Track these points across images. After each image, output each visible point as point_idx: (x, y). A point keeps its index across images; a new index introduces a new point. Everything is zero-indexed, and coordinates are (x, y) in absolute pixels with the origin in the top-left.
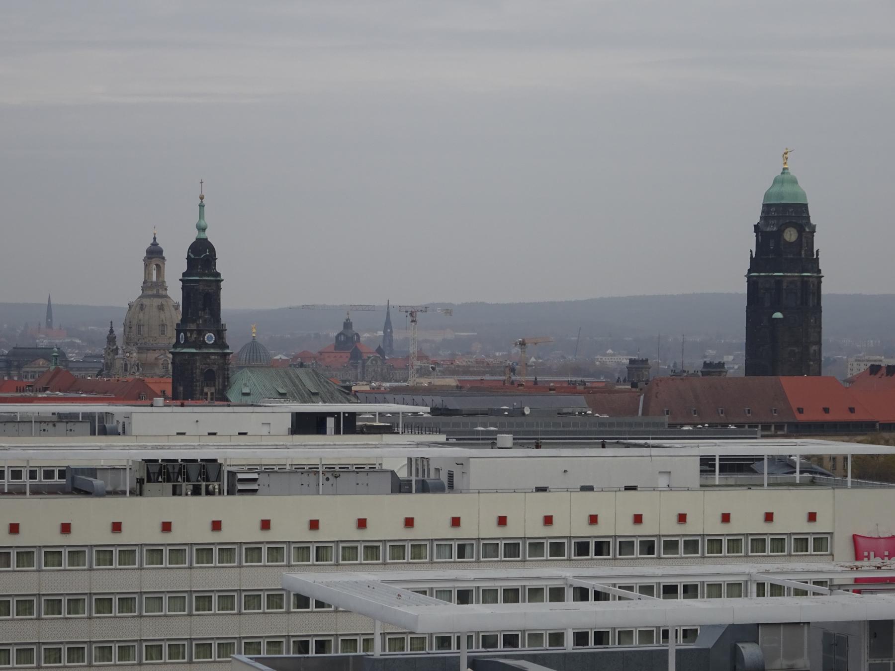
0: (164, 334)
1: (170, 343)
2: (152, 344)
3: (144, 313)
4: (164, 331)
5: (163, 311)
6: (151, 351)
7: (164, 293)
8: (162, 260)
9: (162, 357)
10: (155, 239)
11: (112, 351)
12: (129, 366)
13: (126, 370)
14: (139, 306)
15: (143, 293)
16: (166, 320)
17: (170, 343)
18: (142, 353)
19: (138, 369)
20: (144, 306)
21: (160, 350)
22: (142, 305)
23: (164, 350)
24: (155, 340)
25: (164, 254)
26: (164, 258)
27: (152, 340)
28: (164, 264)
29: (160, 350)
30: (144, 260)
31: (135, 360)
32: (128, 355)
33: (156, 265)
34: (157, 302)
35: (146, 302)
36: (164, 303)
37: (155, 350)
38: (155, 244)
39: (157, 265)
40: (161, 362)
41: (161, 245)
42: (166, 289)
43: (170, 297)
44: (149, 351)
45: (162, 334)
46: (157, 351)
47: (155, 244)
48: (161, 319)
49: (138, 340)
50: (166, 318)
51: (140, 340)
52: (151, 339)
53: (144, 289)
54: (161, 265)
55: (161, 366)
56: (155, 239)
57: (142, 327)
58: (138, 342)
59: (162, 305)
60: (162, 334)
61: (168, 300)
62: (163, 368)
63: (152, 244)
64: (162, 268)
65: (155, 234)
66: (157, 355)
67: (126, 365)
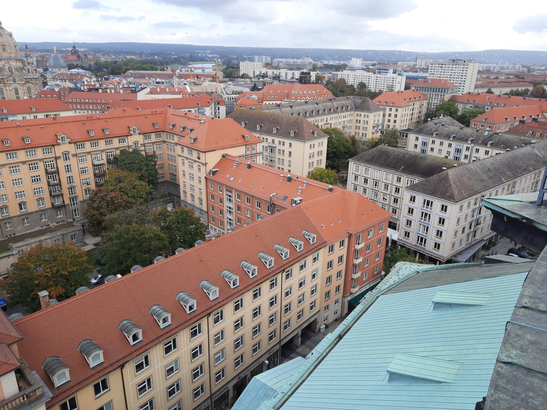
9: (7, 64)
40: (7, 67)
55: (8, 70)
66: (3, 63)
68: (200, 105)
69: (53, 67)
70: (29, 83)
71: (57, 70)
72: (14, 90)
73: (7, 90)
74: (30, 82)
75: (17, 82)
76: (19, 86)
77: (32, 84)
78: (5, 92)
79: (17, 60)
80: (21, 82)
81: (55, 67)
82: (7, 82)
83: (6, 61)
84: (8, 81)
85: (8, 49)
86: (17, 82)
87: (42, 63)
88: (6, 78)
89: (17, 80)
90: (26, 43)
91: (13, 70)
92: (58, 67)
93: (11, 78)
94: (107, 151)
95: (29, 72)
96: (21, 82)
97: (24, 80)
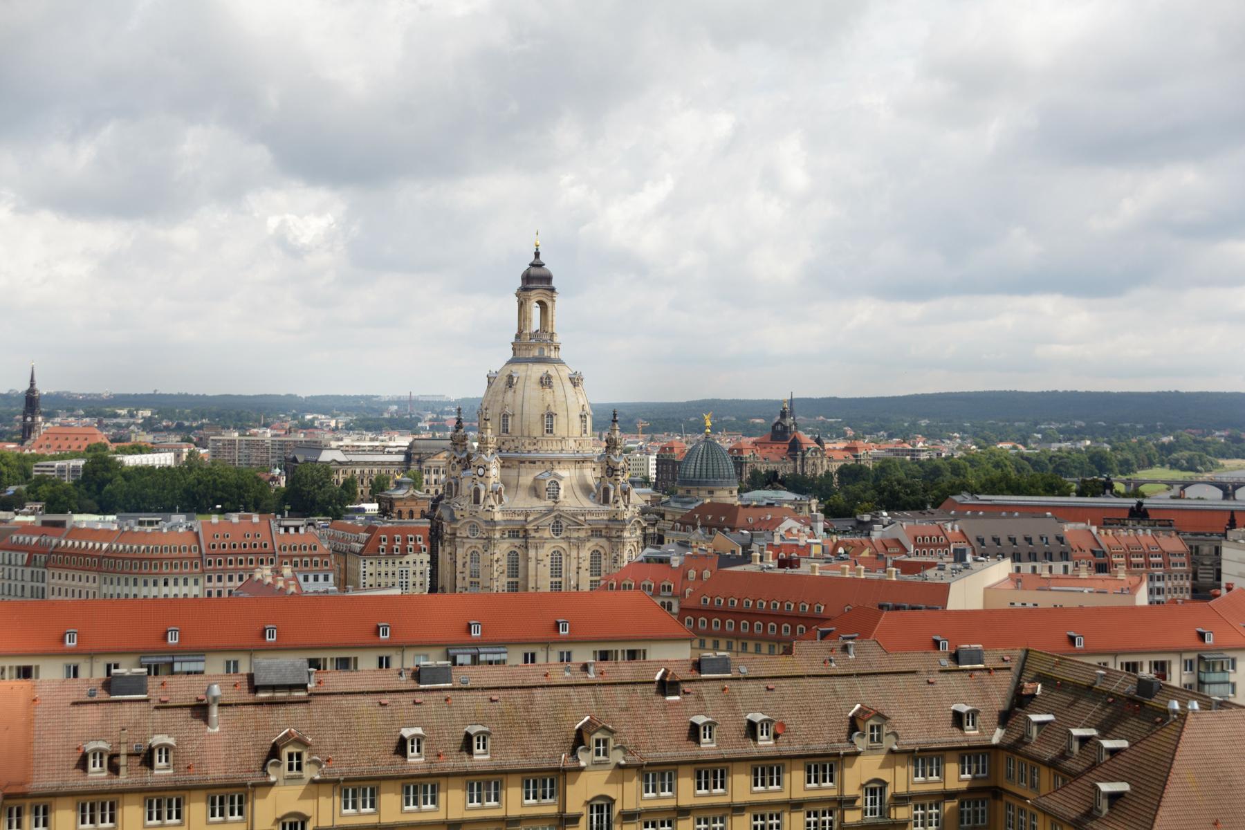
0: (551, 432)
1: (562, 450)
2: (529, 452)
3: (515, 392)
4: (552, 426)
5: (550, 388)
6: (527, 464)
7: (553, 355)
8: (549, 293)
10: (537, 254)
11: (459, 462)
12: (482, 494)
13: (477, 501)
14: (505, 379)
15: (514, 354)
16: (555, 406)
17: (562, 450)
18: (508, 467)
19: (501, 500)
20: (515, 380)
21: (543, 463)
22: (511, 377)
23: (551, 463)
24: (535, 444)
25: (554, 284)
26: (553, 290)
27: (529, 444)
28: (554, 301)
29: (543, 463)
30: (518, 295)
31: (494, 483)
32: (481, 471)
33: (537, 302)
34: (538, 370)
35: (519, 370)
36: (552, 371)
37: (534, 463)
38: (537, 265)
39: (541, 303)
41: (551, 265)
42: (557, 348)
43: (564, 363)
44: (523, 465)
45: (547, 431)
46: (538, 464)
47: (537, 265)
48: (547, 405)
49: (503, 443)
50: (555, 401)
51: (506, 443)
52: (527, 441)
53: (517, 348)
54: (549, 304)
56: (537, 254)
57: (510, 418)
58: (503, 447)
59: (549, 377)
60: (547, 431)
61: (560, 367)
62: (549, 498)
63: (532, 265)
64: (550, 309)
65: (537, 246)
67: (477, 491)
68: (1209, 641)
69: (691, 483)
70: (601, 536)
71: (703, 493)
72: (548, 561)
73: (527, 560)
74: (603, 533)
75: (562, 536)
76: (564, 545)
77: (609, 538)
78: (521, 564)
79: (581, 461)
80: (575, 535)
81: (699, 483)
82: (533, 534)
83: (548, 465)
84: (536, 531)
85: (560, 428)
86: (563, 535)
87: (674, 469)
88: (536, 519)
89: (564, 525)
90: (613, 405)
91: (562, 492)
92: (706, 483)
93: (550, 519)
94: (812, 808)
95: (606, 501)
96: (575, 535)
97: (586, 526)
